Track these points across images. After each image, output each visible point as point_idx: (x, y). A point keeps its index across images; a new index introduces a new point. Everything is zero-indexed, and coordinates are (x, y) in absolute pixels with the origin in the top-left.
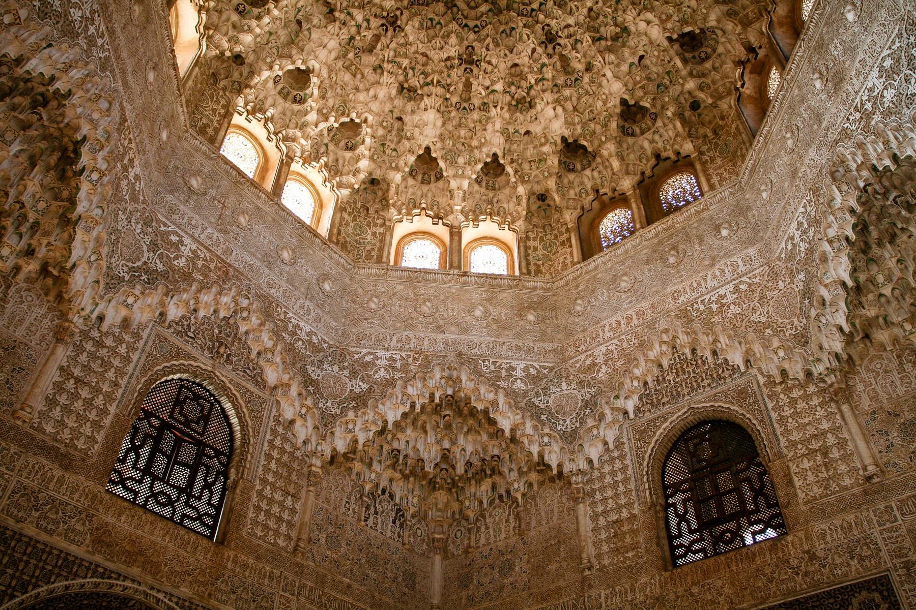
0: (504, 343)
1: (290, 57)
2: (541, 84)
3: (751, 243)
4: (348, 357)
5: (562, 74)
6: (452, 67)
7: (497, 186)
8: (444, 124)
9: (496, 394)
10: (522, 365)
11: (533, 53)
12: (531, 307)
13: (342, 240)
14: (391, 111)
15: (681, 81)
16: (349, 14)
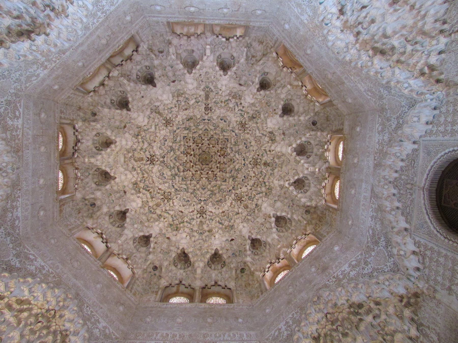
0: (101, 308)
1: (113, 131)
2: (187, 224)
3: (252, 329)
4: (22, 247)
5: (197, 226)
6: (159, 193)
7: (139, 250)
8: (141, 208)
9: (83, 326)
10: (105, 324)
11: (191, 212)
12: (122, 304)
13: (62, 208)
14: (125, 186)
15: (244, 256)
16: (143, 142)
